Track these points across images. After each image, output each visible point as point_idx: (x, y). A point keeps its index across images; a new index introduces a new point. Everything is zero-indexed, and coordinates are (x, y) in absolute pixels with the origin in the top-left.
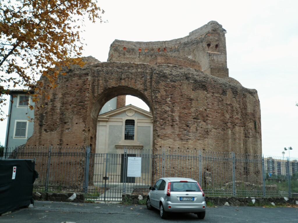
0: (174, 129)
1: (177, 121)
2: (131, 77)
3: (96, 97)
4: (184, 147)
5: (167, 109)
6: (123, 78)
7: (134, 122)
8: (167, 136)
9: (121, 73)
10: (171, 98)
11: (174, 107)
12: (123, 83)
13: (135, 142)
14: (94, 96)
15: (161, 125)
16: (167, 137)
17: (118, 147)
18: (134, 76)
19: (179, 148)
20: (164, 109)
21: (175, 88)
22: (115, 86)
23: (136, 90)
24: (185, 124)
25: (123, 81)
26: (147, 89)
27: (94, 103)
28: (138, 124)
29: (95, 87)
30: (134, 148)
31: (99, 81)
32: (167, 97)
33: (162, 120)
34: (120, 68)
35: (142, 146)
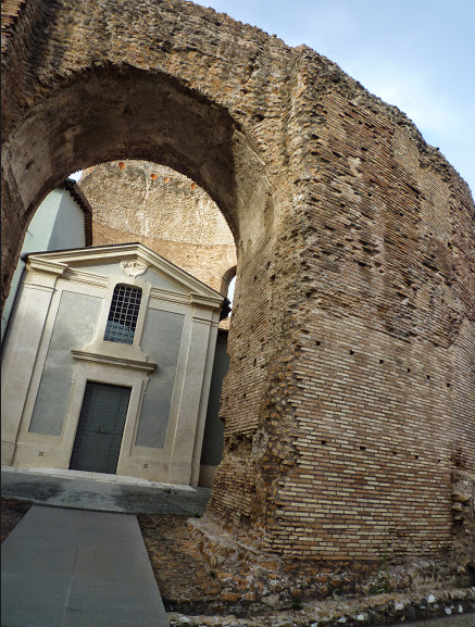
0: (368, 280)
1: (378, 252)
2: (209, 52)
3: (45, 86)
4: (399, 362)
5: (349, 194)
6: (176, 46)
7: (140, 296)
8: (344, 299)
9: (171, 28)
10: (362, 160)
11: (370, 195)
12: (172, 65)
13: (134, 353)
14: (39, 82)
15: (329, 254)
16: (345, 306)
17: (79, 357)
18: (222, 53)
19: (381, 362)
20: (340, 192)
21: (374, 132)
22: (139, 67)
23: (219, 106)
24: (404, 274)
25: (174, 58)
26: (267, 114)
27: (27, 107)
28: (152, 301)
29: (47, 44)
30: (128, 368)
31: (70, 26)
32: (352, 152)
33: (329, 233)
34: (168, 11)
35: (155, 366)
